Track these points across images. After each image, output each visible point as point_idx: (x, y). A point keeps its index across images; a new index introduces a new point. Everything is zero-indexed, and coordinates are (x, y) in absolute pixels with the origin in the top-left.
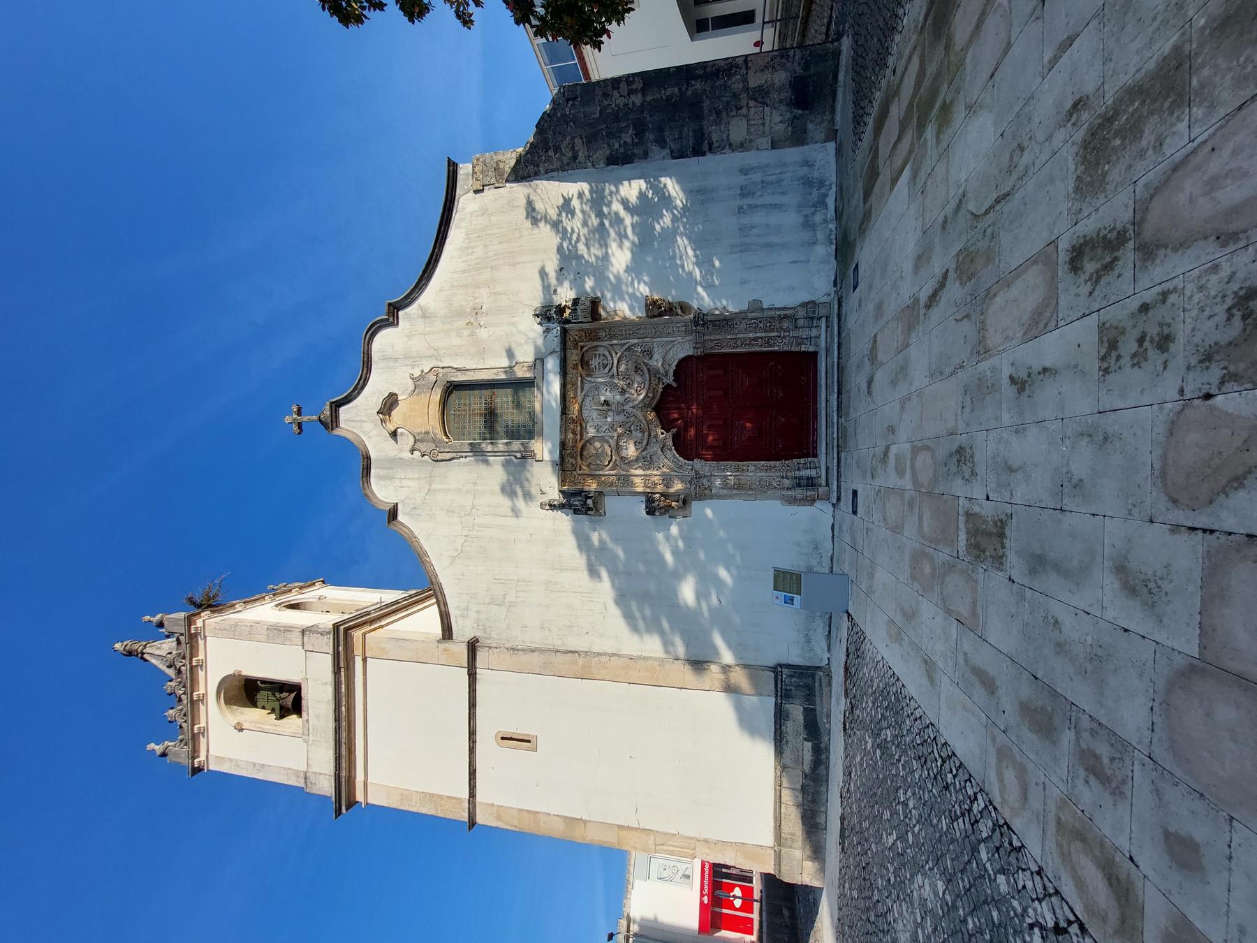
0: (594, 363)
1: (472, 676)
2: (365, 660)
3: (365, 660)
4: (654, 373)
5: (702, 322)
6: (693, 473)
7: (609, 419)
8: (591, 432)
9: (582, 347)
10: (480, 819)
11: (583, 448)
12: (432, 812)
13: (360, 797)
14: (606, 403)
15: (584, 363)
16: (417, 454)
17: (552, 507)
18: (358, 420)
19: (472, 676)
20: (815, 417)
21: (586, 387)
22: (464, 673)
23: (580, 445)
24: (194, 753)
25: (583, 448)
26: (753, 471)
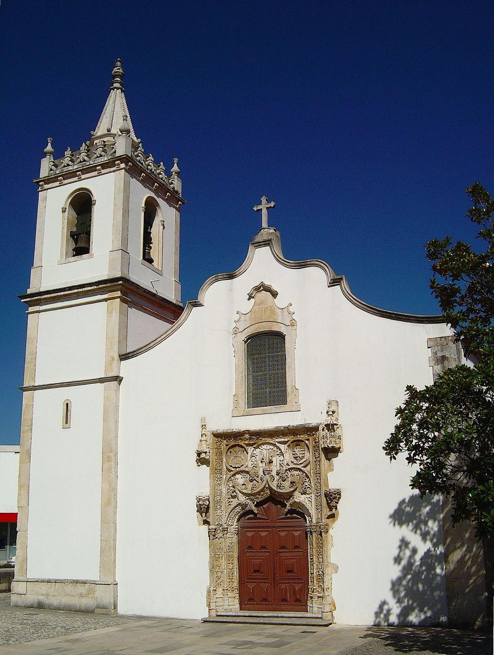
0: (298, 451)
1: (101, 381)
2: (106, 300)
3: (106, 300)
4: (290, 495)
5: (322, 531)
6: (225, 526)
7: (260, 465)
8: (250, 450)
9: (308, 440)
10: (26, 394)
11: (242, 447)
12: (26, 360)
13: (31, 309)
14: (271, 462)
15: (297, 443)
16: (237, 317)
17: (204, 426)
18: (262, 264)
19: (101, 381)
20: (259, 610)
21: (282, 447)
22: (103, 375)
23: (242, 443)
24: (48, 181)
25: (242, 447)
26: (231, 568)
